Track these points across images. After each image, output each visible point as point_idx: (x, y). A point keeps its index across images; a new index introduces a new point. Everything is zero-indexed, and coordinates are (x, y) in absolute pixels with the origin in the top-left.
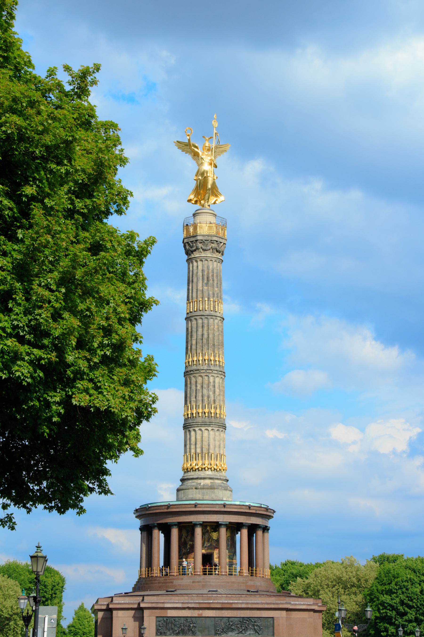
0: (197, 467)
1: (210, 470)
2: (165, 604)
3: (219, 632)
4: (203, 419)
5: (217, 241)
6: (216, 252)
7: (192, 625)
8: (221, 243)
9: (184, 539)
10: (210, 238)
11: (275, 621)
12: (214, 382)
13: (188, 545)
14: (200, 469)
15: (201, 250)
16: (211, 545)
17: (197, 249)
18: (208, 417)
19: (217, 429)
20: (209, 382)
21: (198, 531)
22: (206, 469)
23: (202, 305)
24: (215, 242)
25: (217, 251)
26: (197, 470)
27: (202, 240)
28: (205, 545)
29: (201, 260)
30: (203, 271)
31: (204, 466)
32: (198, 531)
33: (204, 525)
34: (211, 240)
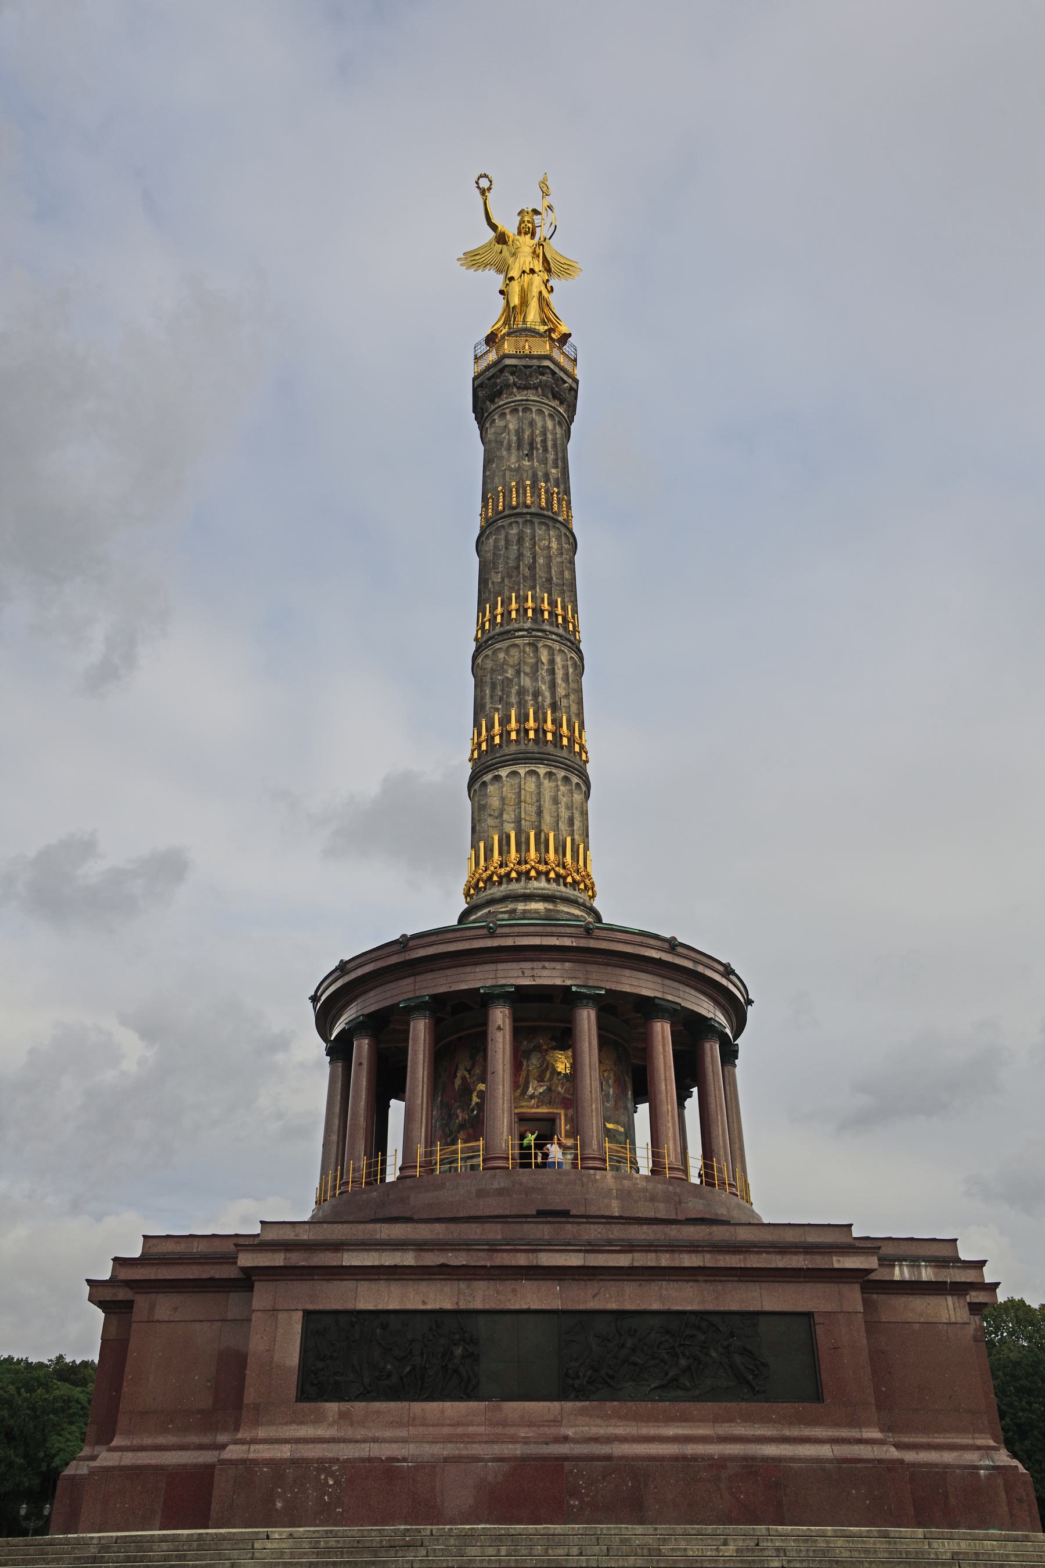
0: (502, 871)
1: (543, 878)
2: (346, 1255)
3: (577, 1383)
4: (522, 747)
5: (553, 373)
6: (550, 396)
7: (459, 1351)
8: (565, 382)
9: (463, 1078)
10: (535, 362)
11: (820, 1331)
12: (552, 662)
13: (475, 1094)
14: (514, 875)
15: (515, 390)
16: (549, 1089)
17: (508, 386)
18: (536, 741)
19: (563, 773)
20: (538, 660)
21: (500, 1016)
22: (533, 873)
23: (518, 497)
24: (548, 371)
25: (555, 397)
26: (504, 880)
27: (516, 366)
28: (531, 1091)
29: (515, 411)
30: (519, 433)
31: (524, 868)
32: (500, 1016)
33: (521, 998)
34: (539, 367)
